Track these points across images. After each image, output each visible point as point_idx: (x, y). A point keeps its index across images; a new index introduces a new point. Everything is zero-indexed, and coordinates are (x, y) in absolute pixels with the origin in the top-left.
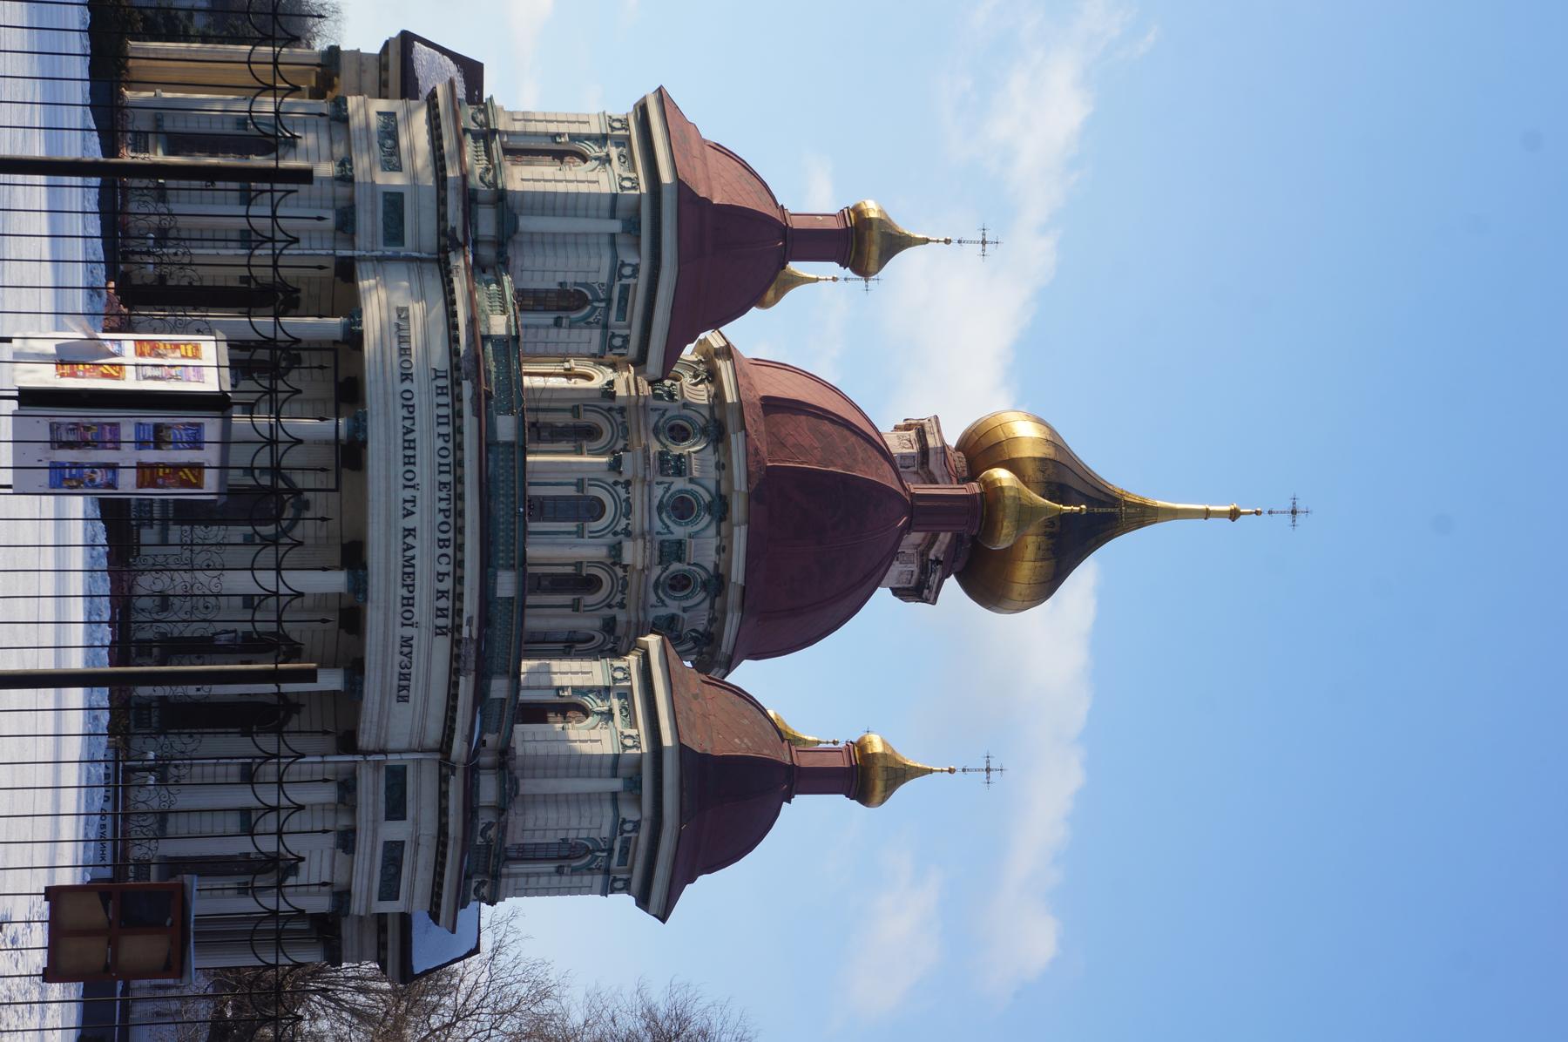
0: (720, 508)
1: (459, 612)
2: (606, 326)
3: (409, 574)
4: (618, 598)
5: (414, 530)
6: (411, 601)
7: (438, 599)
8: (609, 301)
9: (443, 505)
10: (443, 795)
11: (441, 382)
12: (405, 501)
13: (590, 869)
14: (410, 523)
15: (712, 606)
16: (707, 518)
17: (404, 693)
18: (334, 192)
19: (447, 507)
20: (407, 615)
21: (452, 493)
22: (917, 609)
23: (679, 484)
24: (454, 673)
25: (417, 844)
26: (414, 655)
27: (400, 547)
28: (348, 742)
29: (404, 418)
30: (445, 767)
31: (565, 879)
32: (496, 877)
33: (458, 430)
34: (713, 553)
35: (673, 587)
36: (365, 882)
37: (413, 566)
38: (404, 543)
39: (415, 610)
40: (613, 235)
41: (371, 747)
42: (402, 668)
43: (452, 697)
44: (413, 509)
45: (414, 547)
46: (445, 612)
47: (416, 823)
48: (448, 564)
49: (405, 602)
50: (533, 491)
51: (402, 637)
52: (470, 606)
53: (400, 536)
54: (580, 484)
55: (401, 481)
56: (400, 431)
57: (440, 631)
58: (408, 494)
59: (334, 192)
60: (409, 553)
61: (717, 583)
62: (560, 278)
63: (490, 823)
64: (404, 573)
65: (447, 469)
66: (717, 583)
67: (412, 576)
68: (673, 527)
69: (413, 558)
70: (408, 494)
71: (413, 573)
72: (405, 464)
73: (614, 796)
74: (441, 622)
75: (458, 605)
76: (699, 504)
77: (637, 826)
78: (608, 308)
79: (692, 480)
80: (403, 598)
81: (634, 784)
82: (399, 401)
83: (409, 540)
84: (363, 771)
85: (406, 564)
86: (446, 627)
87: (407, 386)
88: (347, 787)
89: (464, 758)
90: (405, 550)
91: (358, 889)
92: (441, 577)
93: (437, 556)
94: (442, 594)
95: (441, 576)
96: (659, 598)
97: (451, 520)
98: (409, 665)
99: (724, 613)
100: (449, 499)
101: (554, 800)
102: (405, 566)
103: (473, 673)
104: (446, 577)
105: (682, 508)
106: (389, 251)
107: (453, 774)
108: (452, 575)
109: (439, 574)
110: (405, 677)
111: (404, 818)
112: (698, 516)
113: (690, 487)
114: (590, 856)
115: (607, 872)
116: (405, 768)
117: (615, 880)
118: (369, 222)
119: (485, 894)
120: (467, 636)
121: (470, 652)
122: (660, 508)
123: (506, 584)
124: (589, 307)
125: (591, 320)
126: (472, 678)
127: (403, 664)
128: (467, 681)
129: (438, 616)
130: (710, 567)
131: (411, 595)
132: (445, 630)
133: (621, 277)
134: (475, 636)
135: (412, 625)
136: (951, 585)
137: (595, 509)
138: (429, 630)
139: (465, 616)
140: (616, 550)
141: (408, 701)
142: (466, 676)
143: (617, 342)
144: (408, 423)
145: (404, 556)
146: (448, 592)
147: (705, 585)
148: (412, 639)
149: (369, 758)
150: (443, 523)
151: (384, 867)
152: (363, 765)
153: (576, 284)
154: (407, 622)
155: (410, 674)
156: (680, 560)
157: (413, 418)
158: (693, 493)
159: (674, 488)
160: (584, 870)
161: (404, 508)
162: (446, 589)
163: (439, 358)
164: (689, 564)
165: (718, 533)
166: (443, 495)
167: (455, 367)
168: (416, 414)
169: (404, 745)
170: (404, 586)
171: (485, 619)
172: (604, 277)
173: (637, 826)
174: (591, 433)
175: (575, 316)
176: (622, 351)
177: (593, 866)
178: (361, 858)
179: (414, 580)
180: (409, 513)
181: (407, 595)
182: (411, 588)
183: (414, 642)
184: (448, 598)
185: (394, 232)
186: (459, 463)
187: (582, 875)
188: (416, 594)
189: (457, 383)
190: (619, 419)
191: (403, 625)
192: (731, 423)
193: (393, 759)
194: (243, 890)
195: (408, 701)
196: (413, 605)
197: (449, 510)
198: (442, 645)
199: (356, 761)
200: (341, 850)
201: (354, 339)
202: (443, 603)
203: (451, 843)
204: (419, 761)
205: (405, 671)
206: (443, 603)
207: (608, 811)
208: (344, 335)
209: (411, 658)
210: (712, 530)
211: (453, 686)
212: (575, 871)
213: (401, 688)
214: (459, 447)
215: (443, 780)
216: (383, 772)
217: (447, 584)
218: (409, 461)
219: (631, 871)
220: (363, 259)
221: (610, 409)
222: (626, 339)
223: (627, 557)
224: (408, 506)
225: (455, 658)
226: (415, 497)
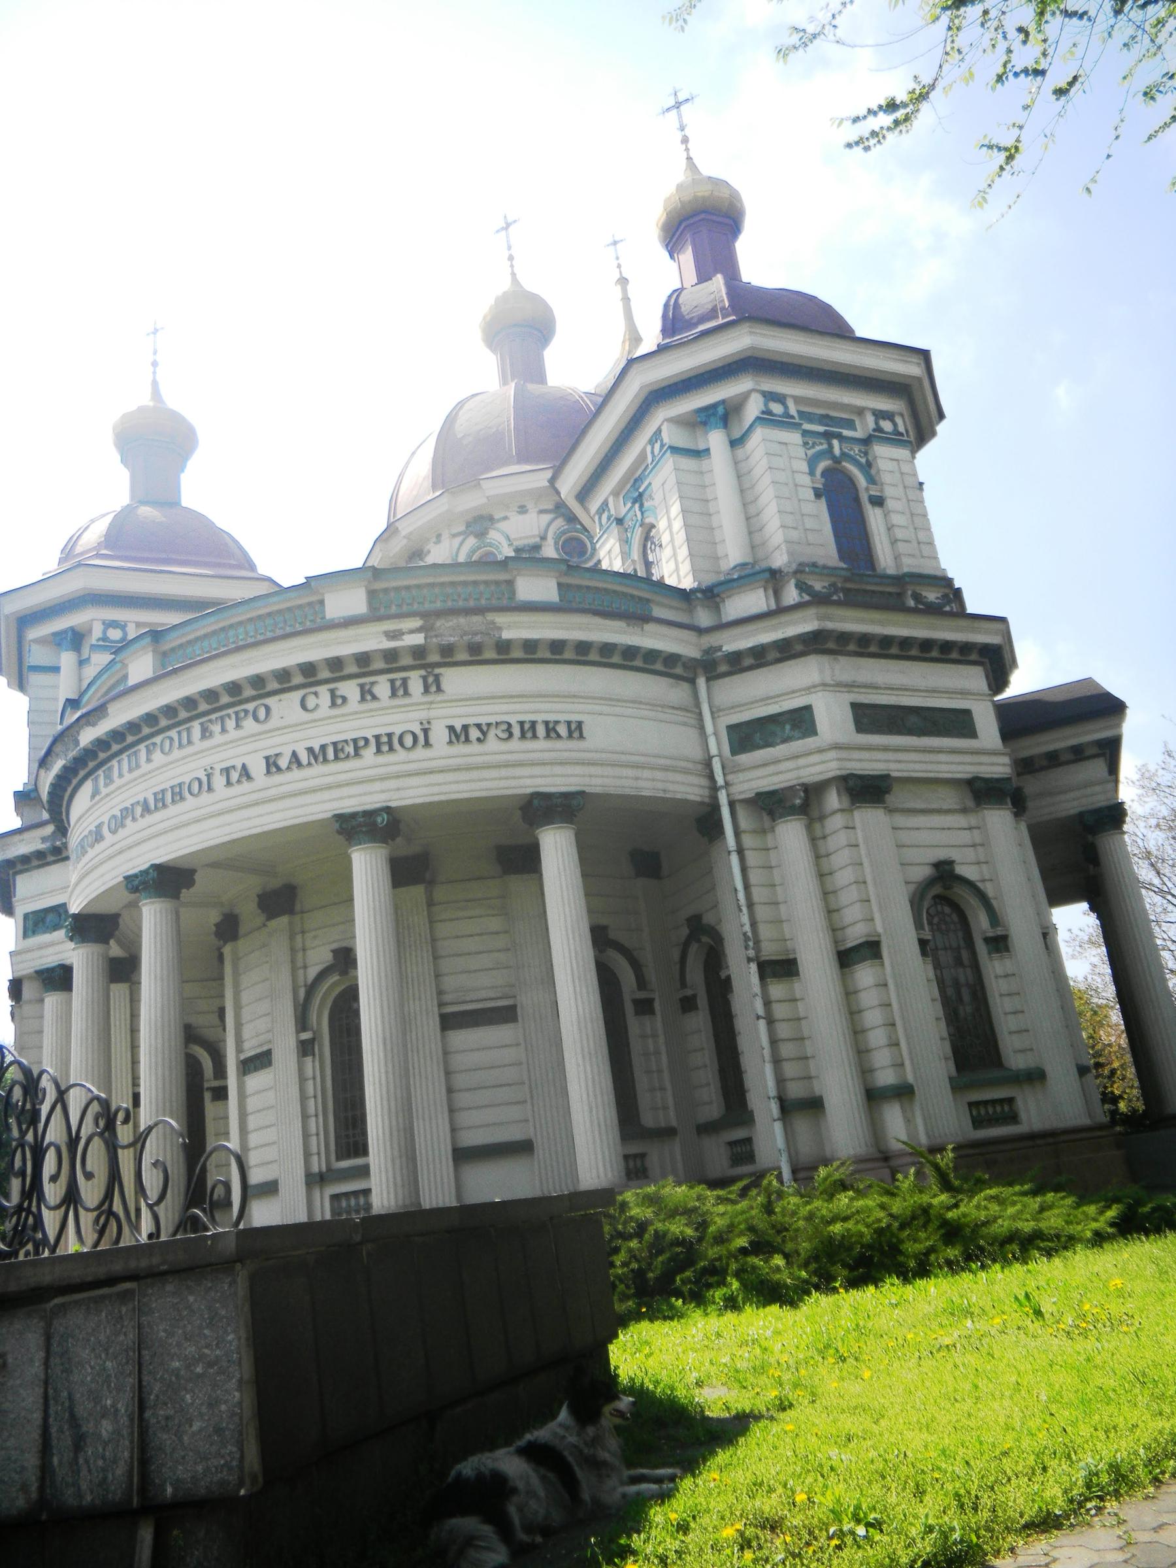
3: (336, 752)
5: (267, 758)
6: (385, 739)
7: (374, 698)
9: (231, 724)
12: (229, 783)
13: (869, 465)
14: (258, 767)
16: (493, 535)
17: (562, 730)
18: (30, 1002)
19: (233, 716)
20: (409, 740)
21: (213, 717)
25: (850, 686)
26: (483, 720)
27: (296, 774)
29: (134, 819)
31: (889, 492)
32: (903, 580)
36: (943, 757)
37: (323, 748)
38: (288, 768)
39: (398, 730)
41: (704, 782)
42: (511, 735)
44: (239, 767)
45: (294, 754)
46: (398, 683)
47: (810, 689)
48: (316, 694)
49: (385, 748)
51: (450, 742)
53: (278, 778)
56: (150, 819)
57: (433, 685)
58: (219, 781)
59: (30, 1002)
60: (304, 757)
63: (797, 586)
64: (336, 758)
65: (184, 735)
67: (340, 747)
69: (310, 750)
70: (219, 781)
71: (335, 744)
72: (182, 799)
75: (379, 664)
76: (479, 548)
77: (770, 396)
80: (379, 751)
82: (122, 833)
83: (283, 763)
84: (746, 786)
85: (321, 759)
86: (425, 679)
90: (299, 765)
91: (960, 768)
92: (339, 701)
93: (306, 716)
94: (367, 694)
95: (336, 700)
97: (250, 706)
98: (505, 727)
100: (222, 718)
102: (325, 760)
103: (490, 616)
104: (338, 693)
107: (720, 648)
108: (332, 686)
109: (334, 704)
110: (528, 730)
111: (808, 709)
112: (490, 545)
114: (844, 464)
115: (867, 441)
116: (731, 728)
117: (878, 429)
119: (939, 595)
120: (422, 635)
126: (500, 619)
127: (505, 735)
128: (509, 627)
129: (406, 693)
130: (546, 518)
131: (373, 741)
132: (431, 679)
134: (417, 623)
135: (426, 731)
138: (431, 703)
141: (580, 724)
142: (500, 629)
144: (139, 810)
145: (309, 764)
146: (362, 686)
148: (451, 729)
149: (720, 781)
150: (256, 719)
151: (911, 732)
152: (733, 790)
155: (522, 723)
160: (873, 472)
161: (239, 781)
162: (358, 690)
164: (544, 538)
165: (505, 518)
166: (216, 728)
169: (693, 734)
170: (357, 754)
177: (863, 460)
178: (893, 766)
179: (346, 741)
180: (245, 773)
181: (373, 748)
182: (362, 743)
184: (373, 683)
187: (878, 471)
188: (369, 734)
191: (427, 744)
194: (1000, 943)
195: (580, 724)
196: (390, 735)
197: (237, 713)
199: (732, 804)
200: (887, 796)
202: (382, 687)
203: (830, 625)
205: (516, 731)
206: (382, 687)
208: (88, 942)
209: (489, 725)
210: (502, 525)
212: (872, 480)
216: (744, 758)
217: (349, 689)
218: (178, 794)
219: (860, 411)
224: (235, 776)
225: (476, 655)
226: (221, 770)
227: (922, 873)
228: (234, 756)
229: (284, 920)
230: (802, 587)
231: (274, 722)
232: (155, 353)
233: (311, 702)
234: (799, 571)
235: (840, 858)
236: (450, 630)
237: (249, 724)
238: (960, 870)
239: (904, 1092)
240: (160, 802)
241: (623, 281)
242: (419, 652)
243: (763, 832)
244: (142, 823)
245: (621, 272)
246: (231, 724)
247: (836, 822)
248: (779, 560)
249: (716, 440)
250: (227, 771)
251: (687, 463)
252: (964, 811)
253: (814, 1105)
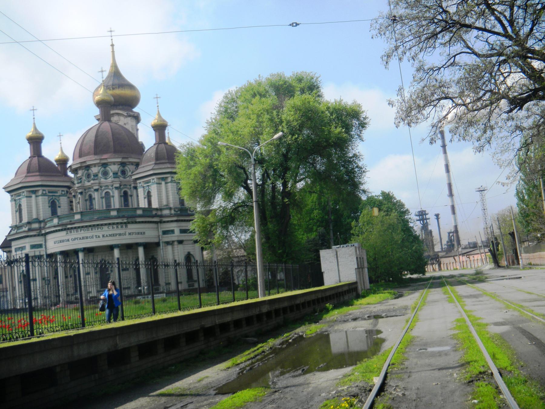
0: (105, 165)
1: (121, 223)
2: (60, 196)
4: (128, 186)
8: (53, 196)
9: (96, 229)
10: (168, 222)
11: (69, 232)
14: (101, 236)
15: (129, 165)
16: (108, 168)
22: (142, 117)
23: (100, 175)
24: (136, 222)
27: (107, 238)
28: (158, 244)
30: (161, 222)
33: (79, 227)
34: (115, 166)
35: (125, 174)
40: (36, 196)
41: (158, 239)
43: (143, 222)
47: (174, 227)
50: (105, 208)
52: (119, 221)
54: (102, 198)
55: (92, 239)
56: (80, 240)
57: (126, 226)
58: (94, 237)
60: (108, 236)
61: (123, 164)
62: (48, 207)
66: (123, 164)
68: (110, 176)
70: (94, 237)
73: (166, 183)
74: (124, 226)
78: (54, 196)
79: (99, 172)
81: (163, 179)
82: (74, 241)
83: (105, 236)
87: (70, 240)
88: (168, 243)
89: (159, 218)
94: (117, 227)
95: (113, 228)
96: (128, 177)
99: (130, 162)
101: (167, 197)
105: (105, 174)
106: (44, 246)
110: (138, 233)
113: (100, 173)
118: (37, 252)
121: (130, 220)
122: (106, 179)
123: (114, 213)
124: (56, 200)
125: (58, 199)
130: (119, 166)
133: (46, 193)
136: (135, 110)
137: (107, 193)
139: (122, 221)
140: (116, 188)
143: (63, 193)
144: (79, 239)
147: (124, 167)
153: (49, 203)
154: (125, 234)
156: (117, 173)
157: (77, 238)
158: (102, 172)
159: (101, 176)
163: (64, 233)
167: (65, 229)
168: (77, 237)
171: (123, 217)
172: (47, 197)
173: (172, 177)
174: (90, 196)
175: (57, 203)
176: (66, 191)
180: (99, 237)
183: (130, 232)
185: (40, 246)
186: (86, 226)
189: (68, 229)
190: (87, 191)
192: (84, 165)
193: (161, 233)
198: (130, 226)
201: (63, 253)
204: (161, 228)
206: (120, 227)
207: (169, 184)
211: (139, 222)
213: (141, 234)
214: (83, 227)
215: (164, 222)
217: (115, 226)
218: (87, 238)
220: (46, 252)
221: (85, 192)
222: (63, 191)
223: (118, 185)
225: (132, 223)
227: (186, 253)
228: (98, 234)
229: (92, 254)
230: (175, 211)
231: (103, 230)
232: (61, 143)
233: (109, 227)
234: (174, 208)
235: (176, 251)
236: (130, 220)
237: (99, 230)
238: (192, 253)
239: (181, 283)
240: (83, 238)
241: (112, 45)
242: (125, 223)
243: (165, 246)
244: (78, 241)
245: (112, 42)
246: (96, 229)
247: (176, 246)
248: (172, 205)
249: (163, 183)
250: (96, 236)
251: (158, 185)
252: (192, 244)
253: (169, 284)
